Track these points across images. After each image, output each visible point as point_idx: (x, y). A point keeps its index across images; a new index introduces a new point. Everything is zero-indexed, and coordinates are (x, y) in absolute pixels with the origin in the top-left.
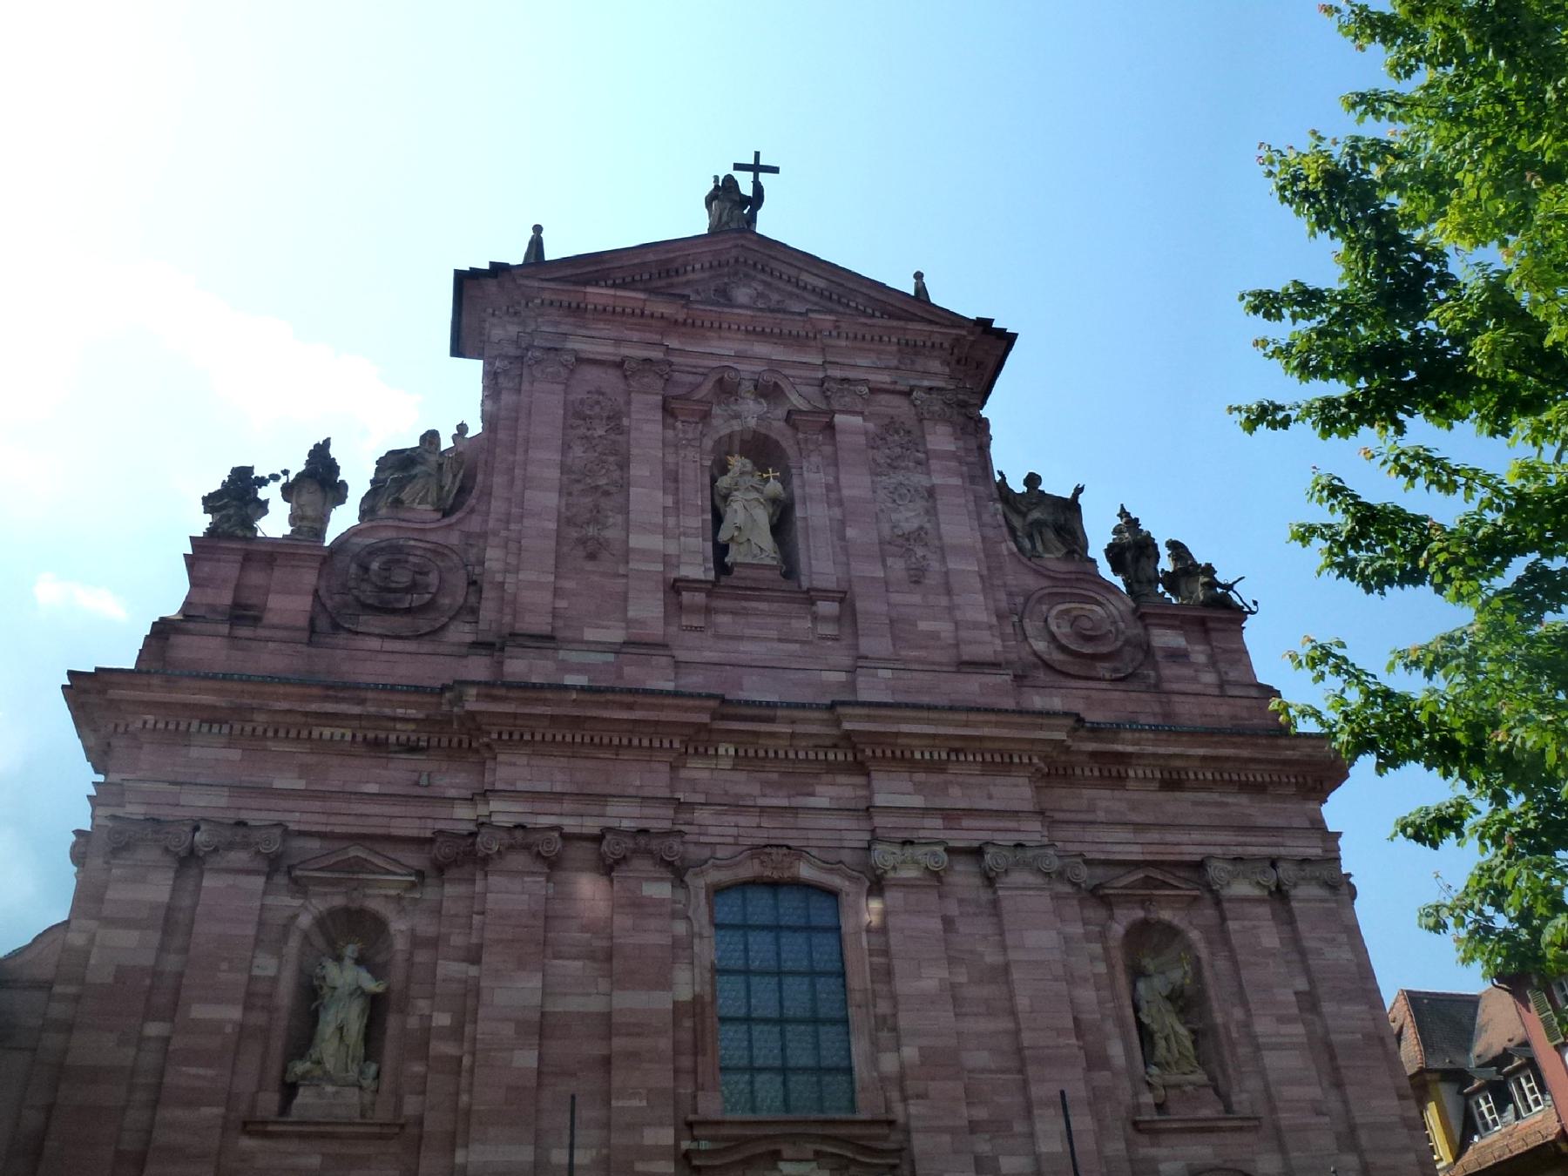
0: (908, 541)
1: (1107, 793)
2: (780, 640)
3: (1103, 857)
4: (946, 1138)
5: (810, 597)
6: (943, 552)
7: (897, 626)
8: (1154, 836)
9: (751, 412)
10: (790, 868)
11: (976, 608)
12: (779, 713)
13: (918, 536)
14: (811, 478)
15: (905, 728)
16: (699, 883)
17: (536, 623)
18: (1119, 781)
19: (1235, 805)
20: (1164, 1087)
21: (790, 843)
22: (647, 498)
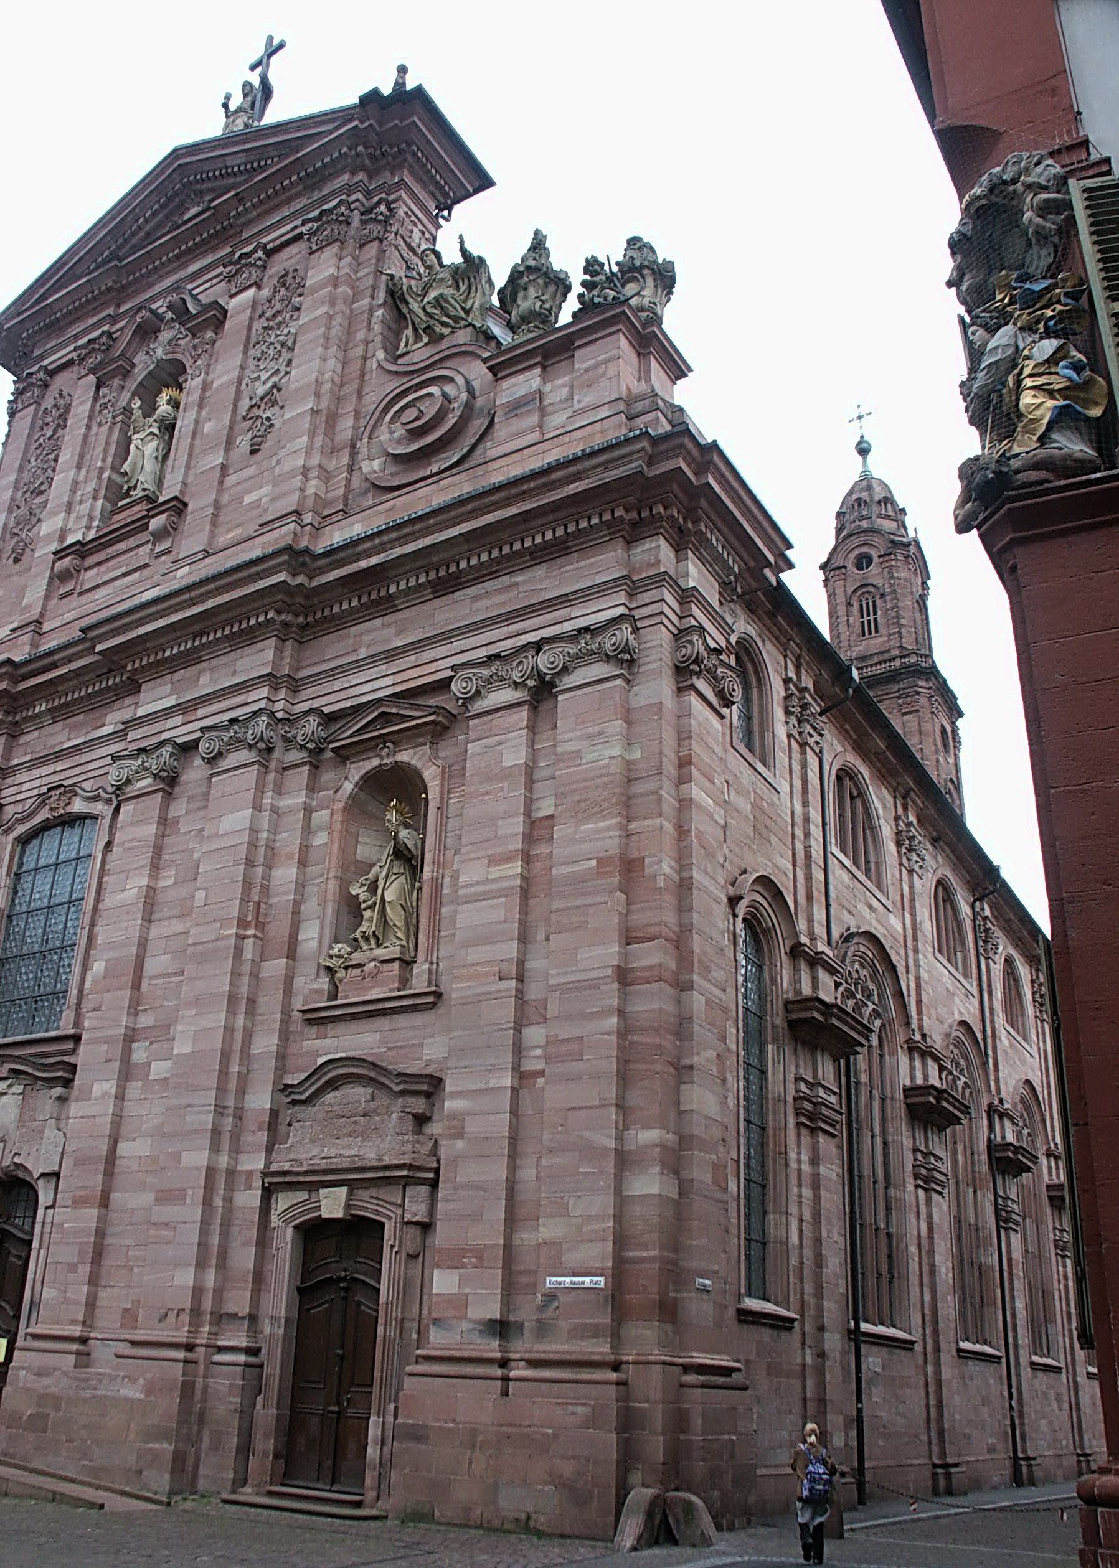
1: (378, 622)
2: (125, 575)
3: (348, 704)
4: (105, 1047)
8: (411, 660)
10: (68, 804)
12: (56, 657)
15: (142, 630)
18: (385, 606)
19: (524, 582)
20: (346, 968)
21: (65, 783)
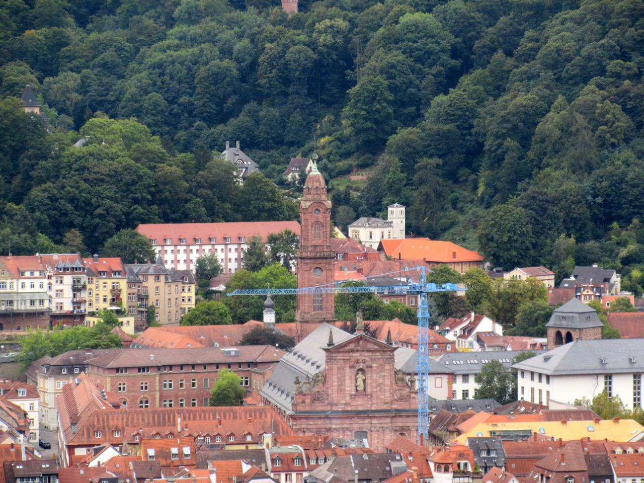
0: (380, 385)
5: (367, 395)
6: (385, 386)
7: (378, 398)
9: (361, 366)
11: (388, 394)
13: (382, 384)
14: (369, 375)
16: (353, 432)
17: (335, 402)
22: (348, 382)
